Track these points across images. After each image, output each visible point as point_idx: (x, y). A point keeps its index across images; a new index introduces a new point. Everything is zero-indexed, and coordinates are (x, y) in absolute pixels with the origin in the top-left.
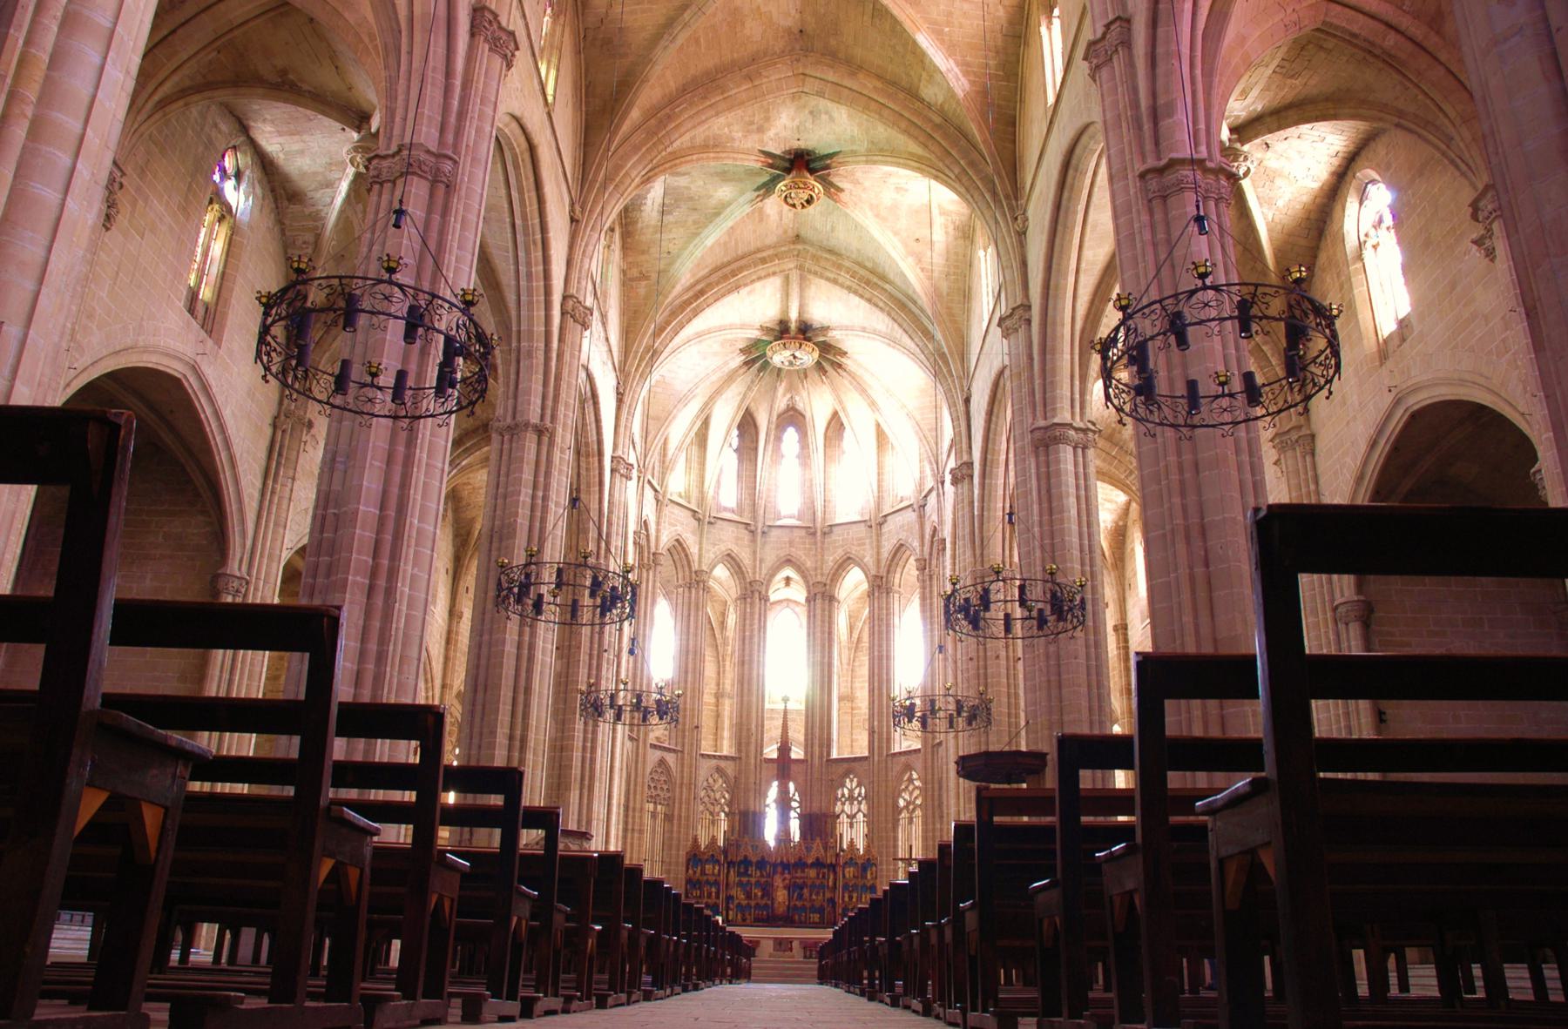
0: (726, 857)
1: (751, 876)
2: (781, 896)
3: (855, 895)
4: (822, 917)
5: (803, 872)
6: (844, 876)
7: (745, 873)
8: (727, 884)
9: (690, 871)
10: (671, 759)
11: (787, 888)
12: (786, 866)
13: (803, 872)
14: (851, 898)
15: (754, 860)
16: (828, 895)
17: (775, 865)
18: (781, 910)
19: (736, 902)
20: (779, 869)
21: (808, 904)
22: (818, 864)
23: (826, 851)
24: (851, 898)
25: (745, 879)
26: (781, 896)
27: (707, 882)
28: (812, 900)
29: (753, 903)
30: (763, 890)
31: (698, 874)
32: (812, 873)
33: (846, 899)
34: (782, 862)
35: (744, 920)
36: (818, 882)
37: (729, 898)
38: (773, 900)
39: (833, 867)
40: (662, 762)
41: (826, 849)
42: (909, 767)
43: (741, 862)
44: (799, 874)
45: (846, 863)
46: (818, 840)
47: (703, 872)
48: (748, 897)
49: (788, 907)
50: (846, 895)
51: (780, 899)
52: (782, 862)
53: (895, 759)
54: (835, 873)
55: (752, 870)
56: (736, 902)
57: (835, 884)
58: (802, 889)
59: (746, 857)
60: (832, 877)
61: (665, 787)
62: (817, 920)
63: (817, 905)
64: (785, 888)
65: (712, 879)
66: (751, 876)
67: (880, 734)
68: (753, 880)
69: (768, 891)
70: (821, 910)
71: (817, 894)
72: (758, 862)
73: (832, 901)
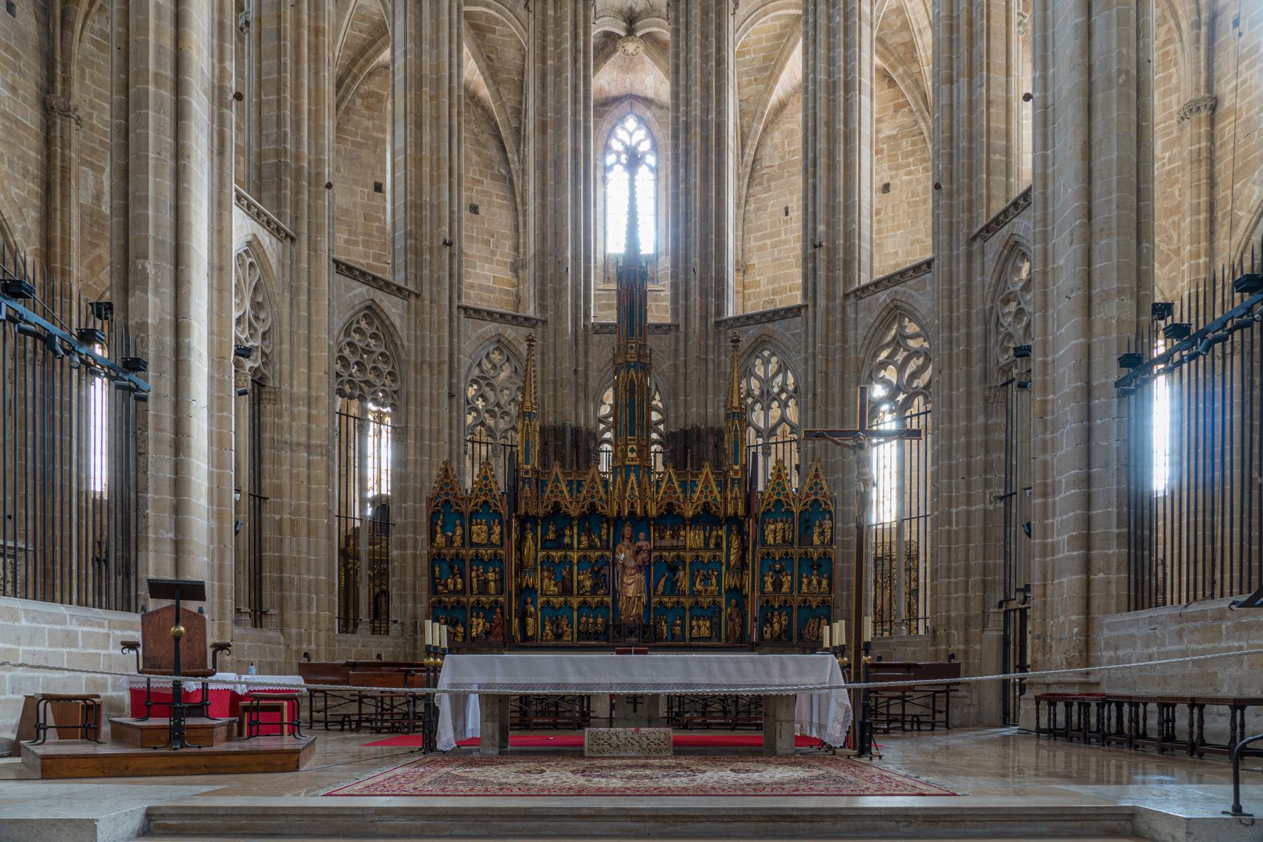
0: (514, 506)
1: (570, 547)
2: (632, 586)
3: (786, 580)
4: (715, 627)
5: (675, 535)
6: (764, 543)
7: (558, 544)
8: (521, 567)
9: (440, 539)
10: (392, 307)
11: (643, 568)
12: (640, 522)
13: (675, 535)
14: (778, 585)
15: (574, 511)
16: (729, 581)
17: (617, 522)
18: (632, 612)
19: (540, 600)
20: (627, 531)
21: (687, 602)
22: (707, 518)
23: (723, 491)
24: (778, 585)
25: (556, 554)
26: (632, 586)
27: (477, 558)
28: (692, 594)
29: (575, 601)
30: (596, 574)
31: (458, 541)
32: (693, 538)
33: (769, 587)
34: (632, 514)
35: (559, 636)
36: (706, 556)
37: (525, 592)
38: (616, 595)
39: (735, 523)
40: (372, 311)
41: (723, 486)
42: (895, 312)
43: (548, 518)
44: (668, 542)
45: (767, 513)
46: (707, 469)
47: (468, 541)
48: (566, 590)
49: (647, 606)
50: (769, 580)
51: (631, 591)
52: (632, 514)
53: (863, 303)
54: (742, 534)
55: (572, 535)
56: (540, 600)
57: (742, 558)
58: (673, 569)
59: (556, 504)
60: (735, 543)
61: (386, 369)
62: (705, 632)
63: (706, 601)
64: (639, 568)
65: (486, 553)
66: (570, 547)
67: (832, 251)
68: (575, 556)
69: (604, 574)
70: (713, 612)
71: (706, 579)
72: (583, 518)
73: (736, 593)
